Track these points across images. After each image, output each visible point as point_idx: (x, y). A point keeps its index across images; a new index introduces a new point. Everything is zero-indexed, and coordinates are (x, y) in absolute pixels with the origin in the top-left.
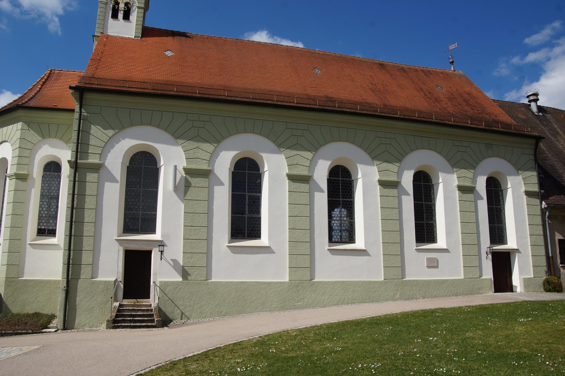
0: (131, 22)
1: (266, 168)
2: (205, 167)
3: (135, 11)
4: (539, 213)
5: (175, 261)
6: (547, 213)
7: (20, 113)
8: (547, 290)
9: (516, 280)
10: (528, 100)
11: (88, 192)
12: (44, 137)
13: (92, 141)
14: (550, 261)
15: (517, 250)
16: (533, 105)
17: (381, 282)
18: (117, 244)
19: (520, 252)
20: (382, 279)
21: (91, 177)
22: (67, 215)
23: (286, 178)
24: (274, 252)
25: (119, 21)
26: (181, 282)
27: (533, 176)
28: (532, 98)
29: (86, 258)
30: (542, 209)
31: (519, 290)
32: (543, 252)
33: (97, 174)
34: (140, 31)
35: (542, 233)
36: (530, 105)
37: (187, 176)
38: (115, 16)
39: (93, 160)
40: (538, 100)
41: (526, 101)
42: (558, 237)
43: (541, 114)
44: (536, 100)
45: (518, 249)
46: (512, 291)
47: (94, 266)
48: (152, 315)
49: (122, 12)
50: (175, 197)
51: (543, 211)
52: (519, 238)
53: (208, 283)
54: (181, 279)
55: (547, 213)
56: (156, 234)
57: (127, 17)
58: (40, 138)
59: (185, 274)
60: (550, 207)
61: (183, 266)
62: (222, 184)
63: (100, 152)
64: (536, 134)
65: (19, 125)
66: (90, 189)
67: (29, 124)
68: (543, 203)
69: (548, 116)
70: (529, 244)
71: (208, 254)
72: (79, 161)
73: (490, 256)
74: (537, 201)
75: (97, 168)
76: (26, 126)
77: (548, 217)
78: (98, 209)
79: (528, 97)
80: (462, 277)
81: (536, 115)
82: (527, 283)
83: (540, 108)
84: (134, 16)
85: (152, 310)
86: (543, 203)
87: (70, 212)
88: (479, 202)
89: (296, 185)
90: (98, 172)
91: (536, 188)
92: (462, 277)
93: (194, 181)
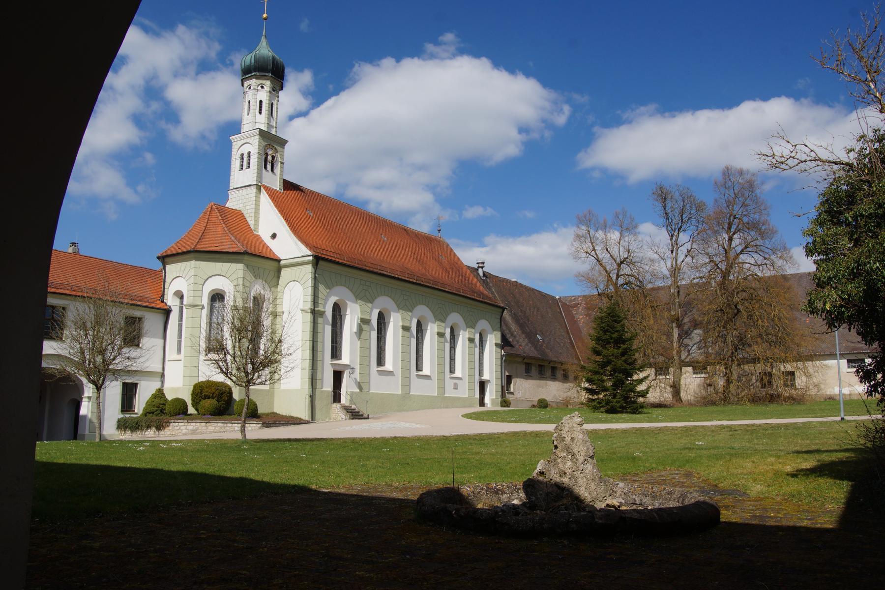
0: (276, 175)
1: (392, 320)
2: (367, 317)
3: (277, 165)
4: (500, 357)
5: (355, 379)
6: (504, 358)
7: (246, 257)
8: (502, 406)
9: (487, 400)
10: (477, 265)
11: (319, 331)
12: (256, 278)
13: (320, 295)
14: (502, 387)
15: (489, 381)
16: (480, 270)
17: (436, 397)
18: (330, 366)
19: (490, 382)
20: (436, 395)
21: (320, 320)
22: (310, 345)
23: (401, 327)
24: (394, 375)
25: (269, 172)
26: (358, 392)
27: (499, 335)
28: (480, 265)
29: (319, 376)
30: (501, 355)
31: (489, 406)
32: (500, 384)
33: (322, 319)
34: (282, 184)
35: (500, 371)
36: (478, 270)
37: (361, 324)
38: (266, 168)
39: (320, 308)
40: (484, 267)
41: (476, 266)
42: (507, 374)
43: (484, 278)
44: (482, 267)
45: (489, 380)
46: (484, 406)
47: (322, 379)
48: (359, 412)
49: (270, 164)
50: (355, 338)
51: (502, 356)
52: (491, 373)
53: (369, 393)
54: (358, 391)
55: (504, 358)
56: (341, 360)
57: (272, 170)
58: (254, 279)
59: (360, 387)
60: (507, 355)
61: (359, 382)
62: (375, 330)
63: (323, 303)
64: (502, 305)
65: (240, 266)
66: (320, 327)
67: (247, 266)
68: (503, 351)
69: (488, 280)
70: (494, 377)
71: (369, 374)
72: (316, 309)
73: (478, 384)
74: (499, 350)
75: (322, 314)
76: (246, 268)
77: (504, 361)
78: (323, 342)
79: (478, 263)
80: (467, 396)
81: (482, 279)
82: (493, 401)
83: (485, 274)
84: (277, 170)
85: (355, 409)
86: (503, 351)
87: (312, 344)
88: (476, 349)
89: (405, 332)
90: (322, 318)
91: (499, 342)
92: (467, 396)
93: (364, 327)
